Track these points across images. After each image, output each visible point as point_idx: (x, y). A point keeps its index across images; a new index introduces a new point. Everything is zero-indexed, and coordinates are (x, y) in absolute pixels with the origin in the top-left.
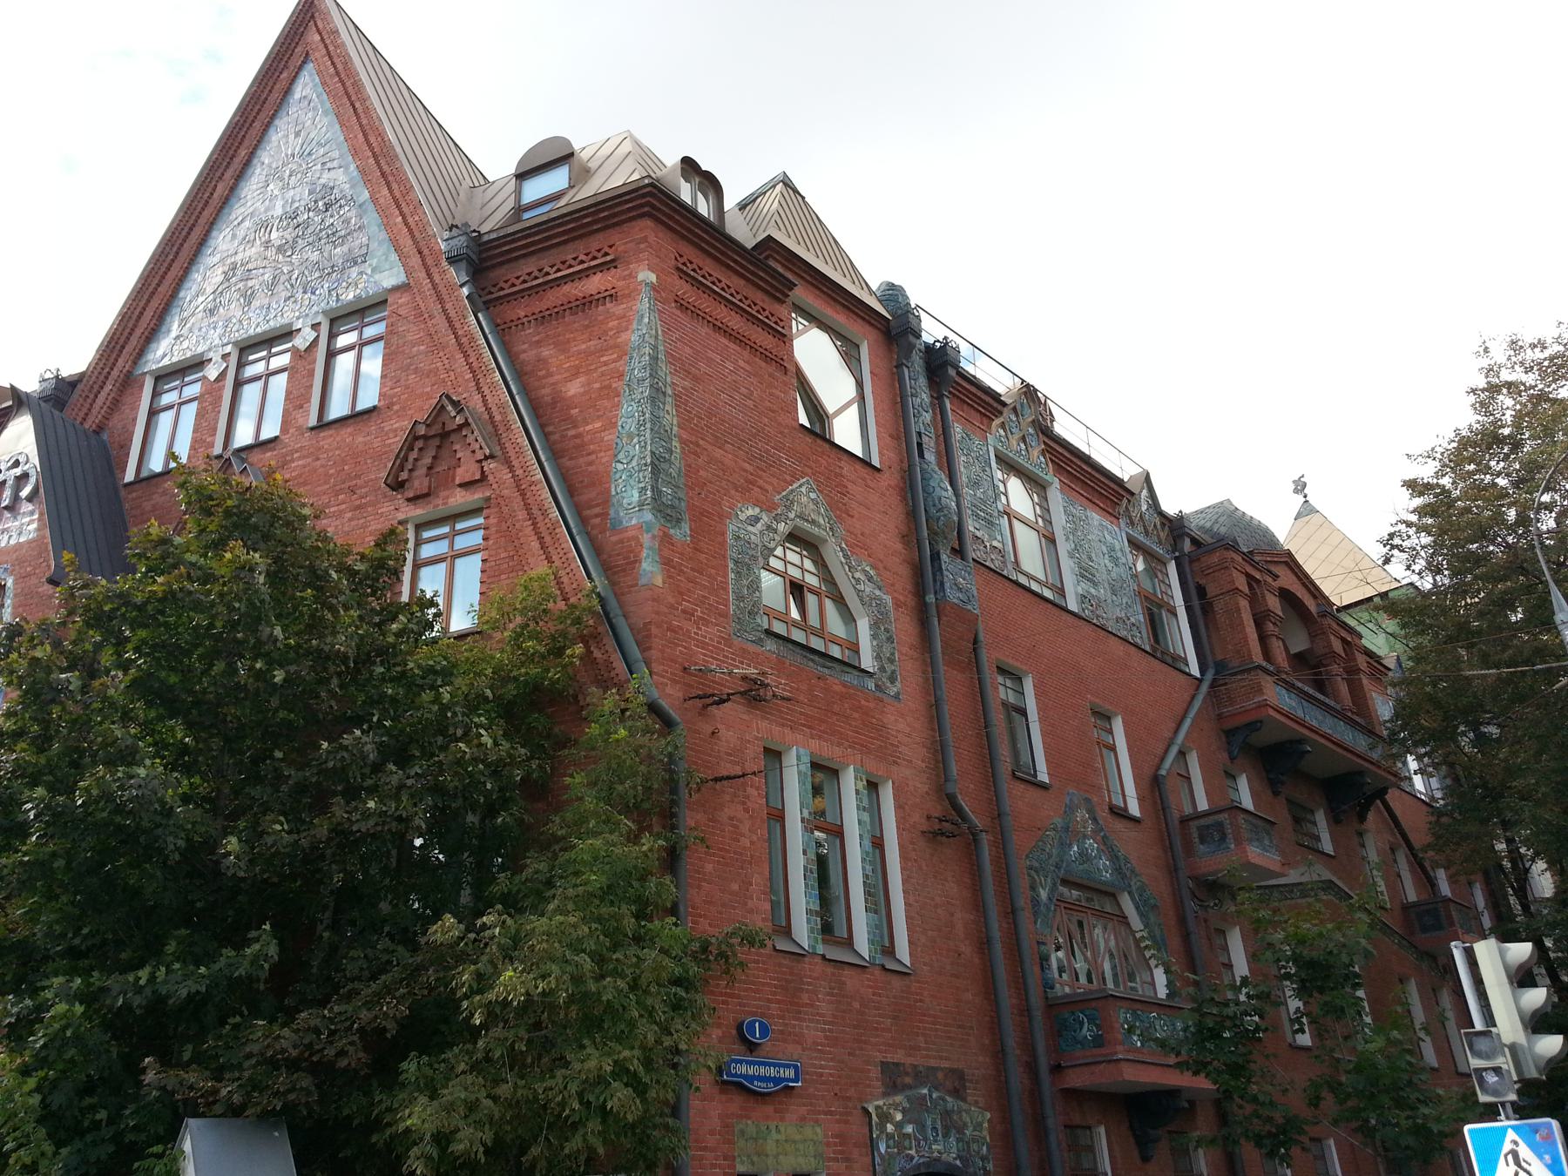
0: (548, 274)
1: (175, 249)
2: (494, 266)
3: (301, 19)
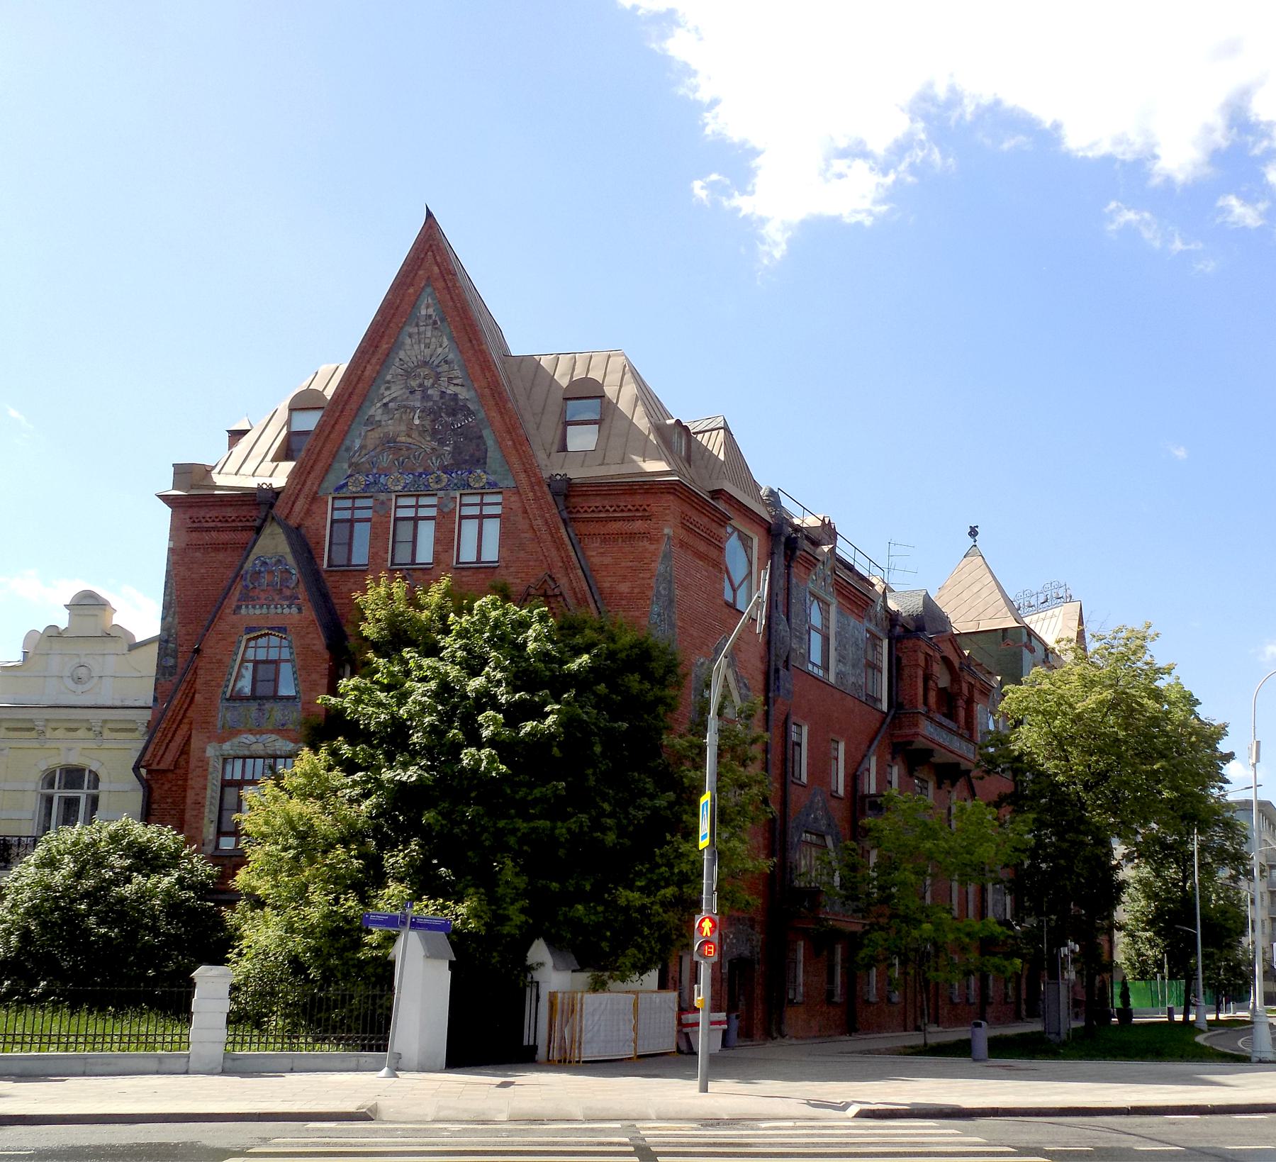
0: (608, 511)
2: (574, 496)
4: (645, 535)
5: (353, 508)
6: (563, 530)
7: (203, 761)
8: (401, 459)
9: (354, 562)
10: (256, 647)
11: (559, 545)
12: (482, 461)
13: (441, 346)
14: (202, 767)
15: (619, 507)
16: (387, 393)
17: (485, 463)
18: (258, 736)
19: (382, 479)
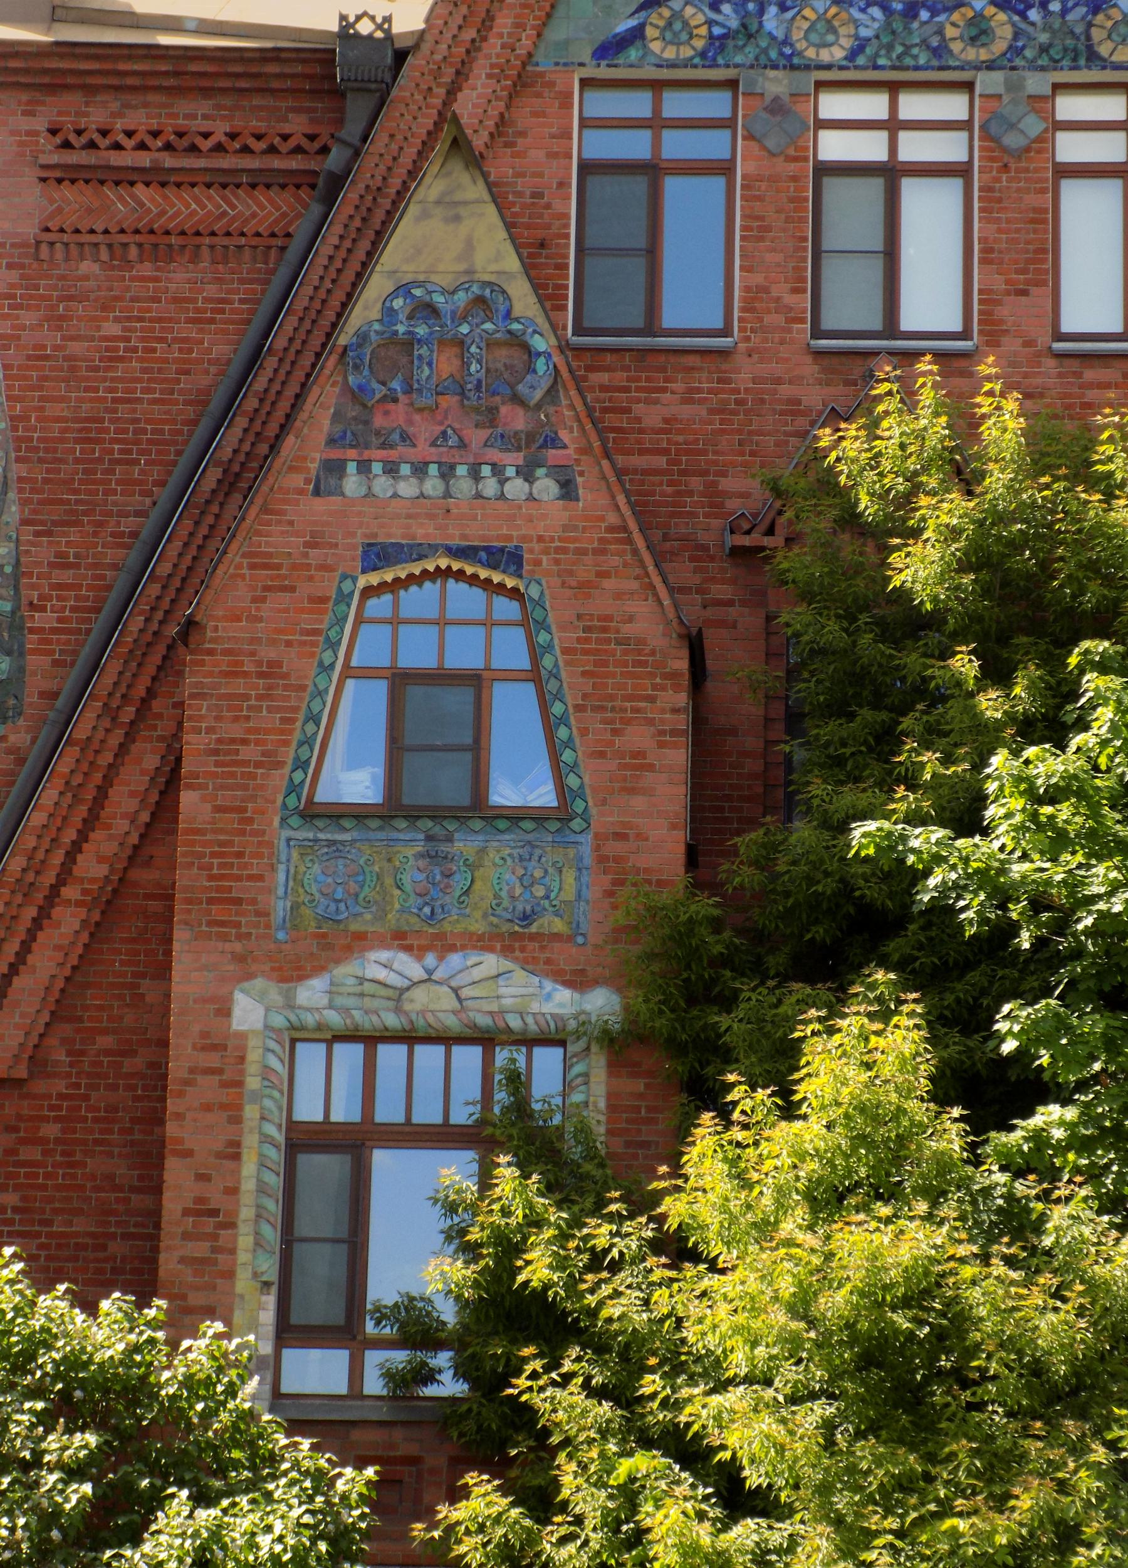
5: (656, 123)
7: (214, 1047)
9: (670, 318)
10: (395, 621)
18: (430, 959)
19: (772, 21)
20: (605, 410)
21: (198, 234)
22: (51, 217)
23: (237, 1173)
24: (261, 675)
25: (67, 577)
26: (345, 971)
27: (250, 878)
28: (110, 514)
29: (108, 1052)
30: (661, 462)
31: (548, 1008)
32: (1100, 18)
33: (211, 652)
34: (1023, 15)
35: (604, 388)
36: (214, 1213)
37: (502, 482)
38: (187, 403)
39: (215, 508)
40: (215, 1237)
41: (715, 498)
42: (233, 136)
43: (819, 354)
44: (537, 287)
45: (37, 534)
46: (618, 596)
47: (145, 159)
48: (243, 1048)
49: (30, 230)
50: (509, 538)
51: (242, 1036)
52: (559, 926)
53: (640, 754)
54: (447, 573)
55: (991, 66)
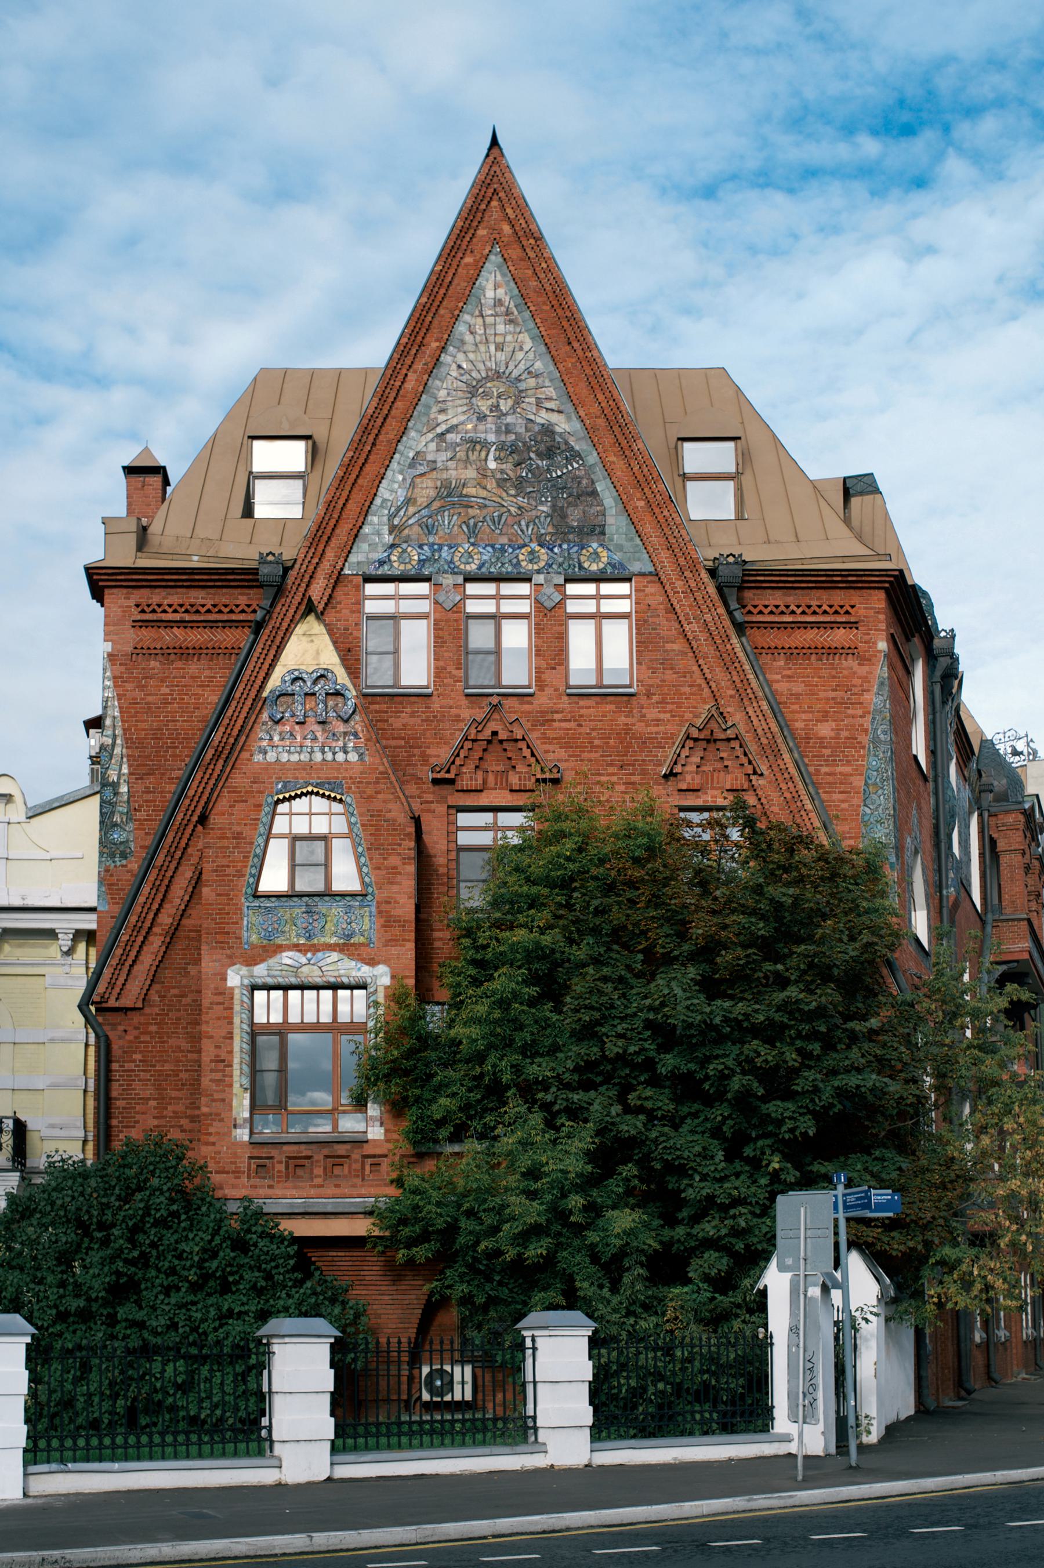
0: (793, 612)
1: (371, 438)
3: (482, 192)
4: (849, 651)
6: (735, 640)
7: (220, 994)
8: (472, 522)
10: (291, 814)
11: (729, 663)
12: (598, 530)
13: (521, 349)
14: (223, 1003)
15: (809, 607)
16: (441, 418)
17: (603, 533)
18: (309, 955)
20: (377, 721)
21: (201, 648)
22: (138, 643)
23: (232, 1044)
24: (234, 838)
25: (150, 797)
26: (272, 962)
27: (233, 923)
28: (167, 770)
29: (175, 996)
30: (402, 743)
31: (359, 974)
32: (584, 551)
33: (212, 829)
34: (552, 550)
35: (376, 712)
36: (223, 1061)
37: (334, 754)
38: (198, 721)
39: (212, 766)
40: (224, 1071)
41: (425, 758)
42: (214, 606)
43: (467, 695)
44: (347, 668)
45: (137, 779)
46: (384, 802)
47: (177, 617)
48: (232, 994)
49: (129, 649)
50: (338, 778)
51: (232, 988)
52: (362, 940)
53: (395, 868)
54: (312, 793)
55: (538, 572)
